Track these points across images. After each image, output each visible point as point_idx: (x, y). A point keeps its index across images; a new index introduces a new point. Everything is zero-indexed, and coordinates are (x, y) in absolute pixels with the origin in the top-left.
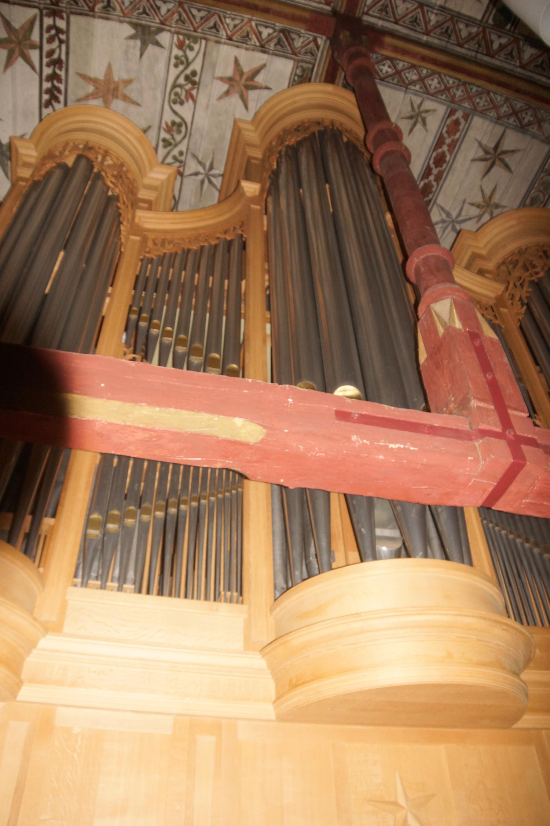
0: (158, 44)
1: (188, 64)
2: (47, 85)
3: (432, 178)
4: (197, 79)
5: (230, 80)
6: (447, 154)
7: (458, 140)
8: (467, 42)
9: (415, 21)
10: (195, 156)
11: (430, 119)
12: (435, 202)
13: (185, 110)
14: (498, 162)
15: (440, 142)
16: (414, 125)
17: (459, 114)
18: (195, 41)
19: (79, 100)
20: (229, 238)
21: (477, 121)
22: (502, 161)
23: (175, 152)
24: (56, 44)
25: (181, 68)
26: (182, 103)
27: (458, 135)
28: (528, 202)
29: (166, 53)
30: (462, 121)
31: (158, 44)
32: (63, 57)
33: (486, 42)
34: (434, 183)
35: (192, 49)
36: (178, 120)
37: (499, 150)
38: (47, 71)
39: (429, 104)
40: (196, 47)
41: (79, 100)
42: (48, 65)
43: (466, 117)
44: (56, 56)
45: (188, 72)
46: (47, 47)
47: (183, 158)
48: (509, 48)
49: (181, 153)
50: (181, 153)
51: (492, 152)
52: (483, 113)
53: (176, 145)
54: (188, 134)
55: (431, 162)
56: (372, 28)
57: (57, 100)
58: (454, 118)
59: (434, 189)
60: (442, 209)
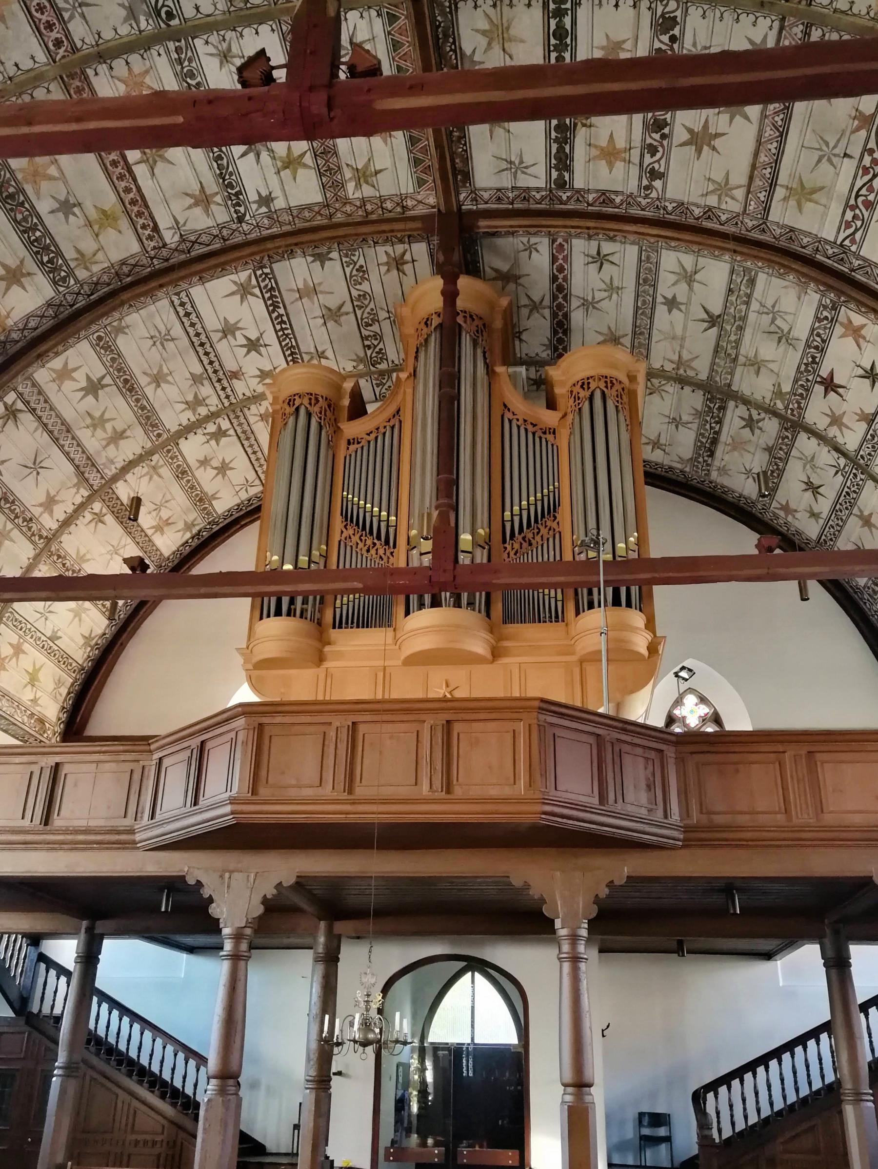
0: (331, 259)
1: (355, 263)
2: (269, 302)
3: (560, 280)
4: (365, 269)
5: (387, 263)
9: (499, 199)
10: (382, 309)
13: (365, 286)
15: (554, 259)
16: (531, 253)
17: (560, 240)
18: (355, 250)
19: (292, 303)
20: (391, 423)
21: (575, 241)
22: (608, 260)
23: (368, 310)
24: (267, 280)
25: (351, 266)
26: (360, 284)
27: (566, 252)
29: (339, 262)
31: (331, 259)
32: (274, 285)
33: (556, 197)
35: (354, 255)
36: (362, 293)
37: (602, 255)
38: (267, 295)
39: (533, 240)
40: (357, 253)
41: (292, 303)
42: (266, 292)
44: (269, 286)
45: (357, 267)
46: (262, 285)
48: (575, 197)
50: (372, 310)
52: (578, 236)
53: (367, 307)
54: (372, 298)
55: (555, 271)
56: (470, 212)
57: (279, 307)
58: (558, 243)
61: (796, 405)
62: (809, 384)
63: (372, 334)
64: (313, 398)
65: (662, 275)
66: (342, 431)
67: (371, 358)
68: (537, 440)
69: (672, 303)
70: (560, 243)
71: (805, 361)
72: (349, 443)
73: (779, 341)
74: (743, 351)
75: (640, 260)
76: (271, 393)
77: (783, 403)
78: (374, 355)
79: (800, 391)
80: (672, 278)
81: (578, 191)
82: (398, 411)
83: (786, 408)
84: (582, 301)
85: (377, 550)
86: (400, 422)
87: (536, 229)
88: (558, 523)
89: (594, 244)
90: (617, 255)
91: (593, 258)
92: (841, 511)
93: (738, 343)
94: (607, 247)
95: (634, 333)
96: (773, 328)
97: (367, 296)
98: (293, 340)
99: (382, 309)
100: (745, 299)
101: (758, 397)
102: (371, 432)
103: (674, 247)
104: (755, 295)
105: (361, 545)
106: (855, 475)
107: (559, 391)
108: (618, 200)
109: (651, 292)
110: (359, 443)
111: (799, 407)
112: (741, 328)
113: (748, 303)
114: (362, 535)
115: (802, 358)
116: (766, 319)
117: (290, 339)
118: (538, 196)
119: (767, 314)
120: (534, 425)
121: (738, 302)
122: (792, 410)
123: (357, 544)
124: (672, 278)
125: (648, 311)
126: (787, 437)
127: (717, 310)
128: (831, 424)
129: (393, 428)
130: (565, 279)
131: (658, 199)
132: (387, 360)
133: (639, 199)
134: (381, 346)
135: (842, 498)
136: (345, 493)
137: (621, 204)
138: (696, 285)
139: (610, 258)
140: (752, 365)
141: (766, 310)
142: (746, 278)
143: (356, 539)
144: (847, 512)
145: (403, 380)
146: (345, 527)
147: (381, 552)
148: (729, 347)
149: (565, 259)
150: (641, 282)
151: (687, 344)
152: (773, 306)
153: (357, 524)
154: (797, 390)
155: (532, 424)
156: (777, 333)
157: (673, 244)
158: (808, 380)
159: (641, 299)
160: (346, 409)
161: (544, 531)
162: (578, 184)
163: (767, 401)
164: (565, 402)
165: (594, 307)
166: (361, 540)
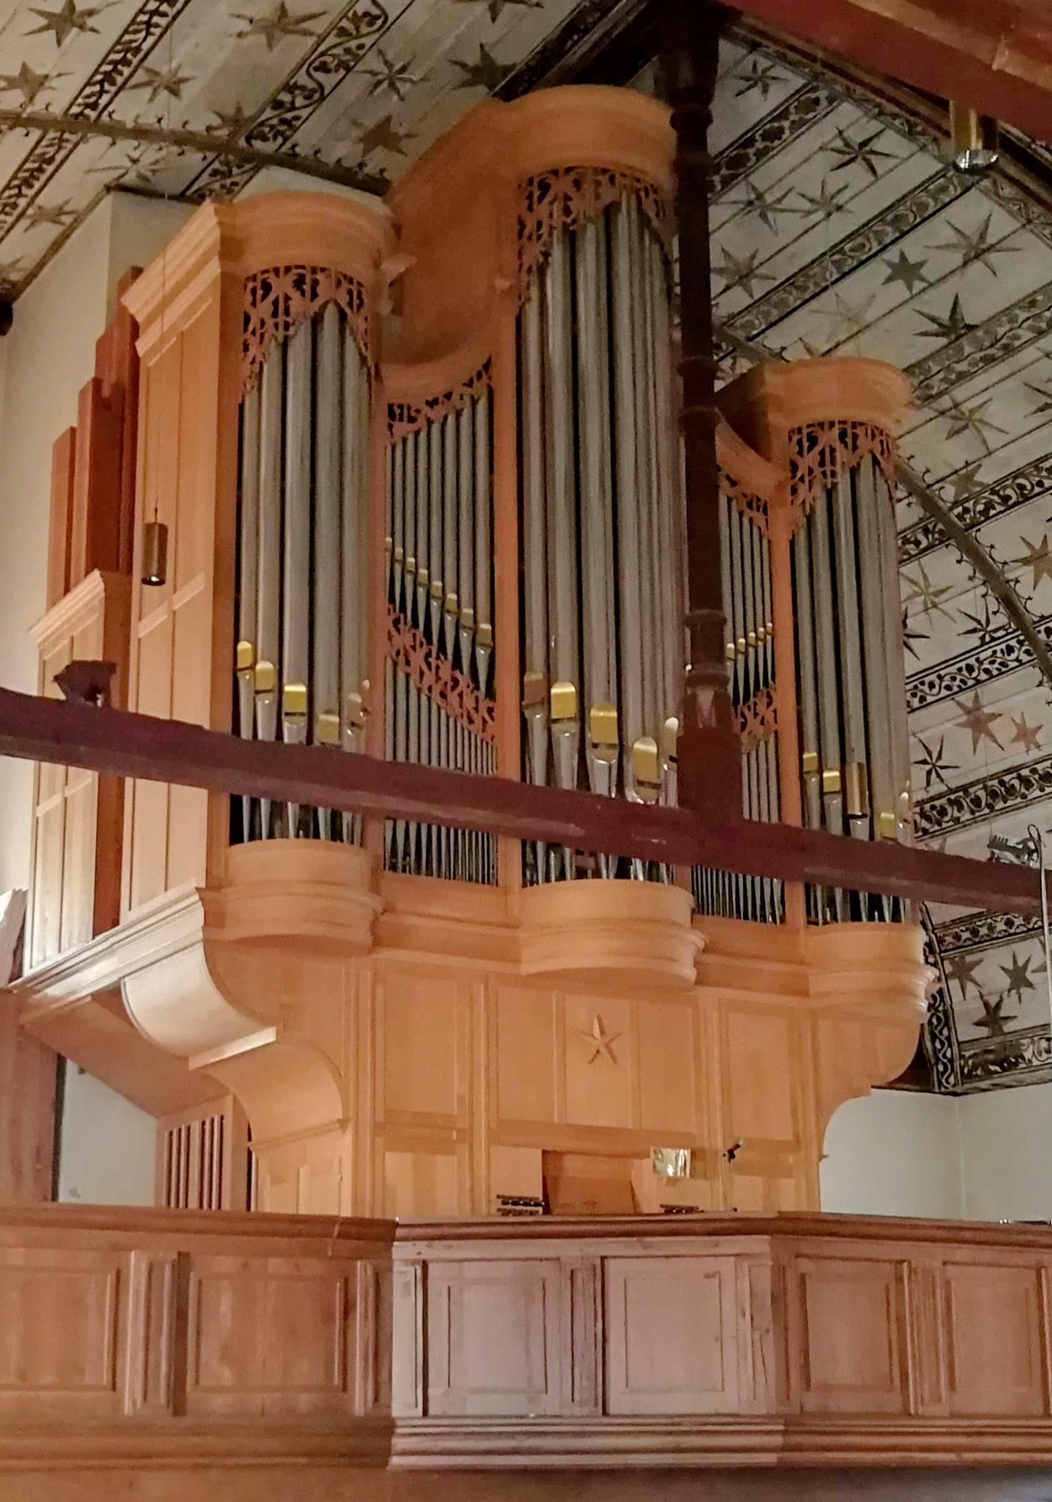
3: (751, 151)
6: (787, 133)
7: (809, 120)
11: (774, 88)
17: (822, 94)
23: (353, 44)
27: (811, 115)
30: (824, 103)
34: (754, 158)
43: (831, 100)
49: (361, 47)
51: (856, 147)
52: (859, 102)
59: (749, 164)
61: (980, 507)
62: (1037, 490)
63: (311, 85)
64: (354, 288)
67: (262, 124)
68: (735, 516)
69: (905, 271)
73: (1041, 410)
74: (959, 393)
75: (923, 186)
76: (220, 224)
77: (957, 494)
78: (275, 121)
79: (1009, 492)
80: (949, 236)
82: (487, 366)
83: (956, 504)
84: (753, 196)
85: (461, 695)
87: (798, 57)
88: (775, 711)
89: (875, 126)
90: (891, 162)
92: (932, 685)
93: (962, 376)
94: (891, 142)
95: (790, 281)
98: (151, 40)
100: (1043, 325)
101: (918, 466)
105: (429, 677)
106: (1010, 650)
107: (775, 419)
109: (888, 240)
110: (412, 420)
111: (985, 513)
112: (990, 360)
114: (428, 655)
117: (148, 33)
120: (734, 483)
121: (1025, 325)
122: (966, 510)
123: (422, 674)
124: (949, 236)
125: (851, 263)
126: (917, 543)
127: (972, 314)
128: (1025, 561)
129: (474, 402)
130: (761, 154)
132: (286, 139)
134: (304, 113)
135: (953, 669)
138: (977, 265)
140: (954, 418)
143: (417, 658)
144: (944, 693)
146: (396, 623)
147: (469, 702)
148: (941, 375)
149: (795, 125)
151: (862, 338)
153: (415, 624)
154: (1005, 488)
155: (728, 478)
157: (1008, 190)
158: (1040, 484)
159: (860, 240)
161: (753, 723)
163: (929, 479)
164: (781, 446)
165: (763, 216)
166: (429, 665)
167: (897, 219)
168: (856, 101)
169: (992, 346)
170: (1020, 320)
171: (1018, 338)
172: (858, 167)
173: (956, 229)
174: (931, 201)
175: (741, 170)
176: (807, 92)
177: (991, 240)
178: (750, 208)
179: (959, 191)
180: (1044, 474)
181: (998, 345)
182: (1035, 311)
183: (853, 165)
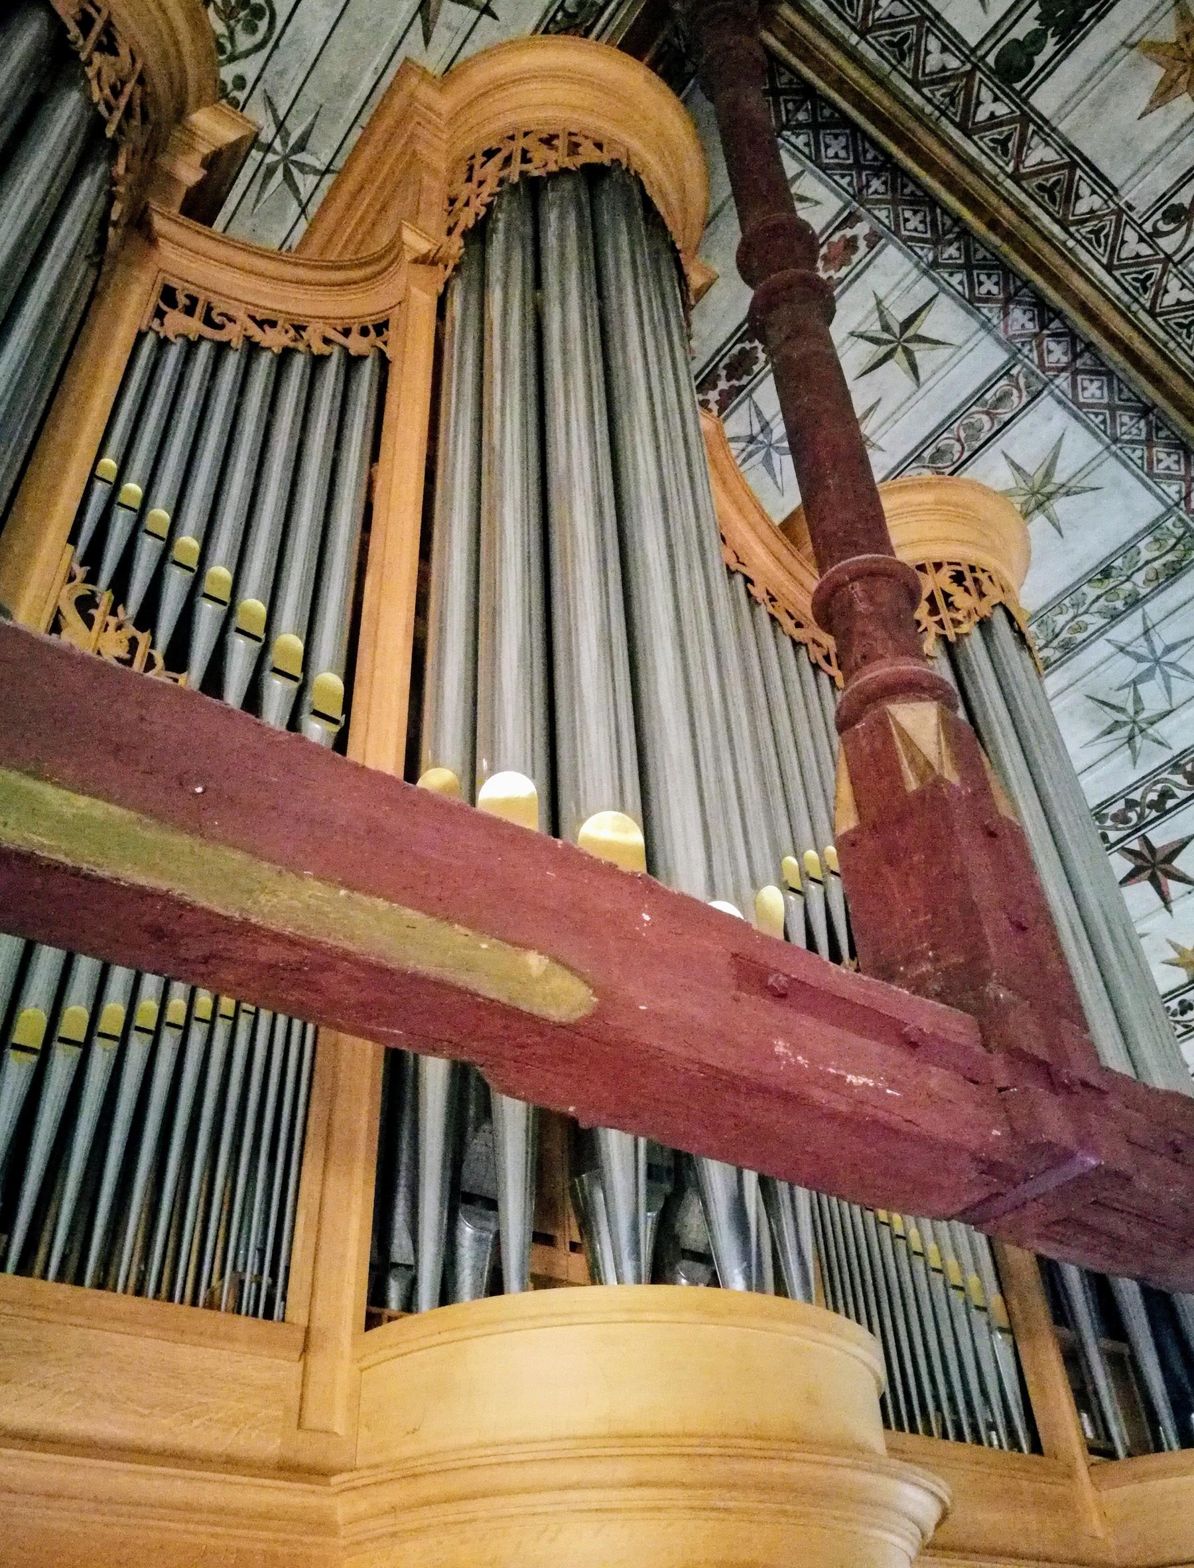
8: (932, 82)
10: (269, 102)
12: (749, 395)
14: (900, 355)
17: (861, 229)
21: (892, 256)
22: (908, 353)
28: (927, 454)
30: (862, 245)
43: (873, 240)
47: (241, 96)
49: (240, 82)
50: (240, 82)
51: (896, 329)
53: (233, 58)
59: (756, 368)
60: (759, 414)
65: (992, 454)
66: (151, 239)
70: (854, 239)
71: (1136, 796)
72: (168, 295)
73: (1109, 732)
75: (977, 397)
81: (1025, 119)
84: (757, 428)
86: (384, 364)
89: (925, 288)
90: (942, 353)
91: (886, 328)
96: (1124, 698)
97: (263, 25)
99: (269, 102)
100: (1119, 604)
102: (273, 324)
103: (1080, 406)
104: (1154, 609)
108: (1088, 202)
113: (1115, 617)
115: (1133, 788)
116: (1127, 668)
118: (934, 61)
119: (1139, 659)
131: (1168, 258)
133: (1130, 235)
136: (109, 464)
137: (1082, 222)
139: (921, 353)
141: (1144, 650)
142: (1170, 557)
145: (408, 257)
150: (927, 454)
152: (1169, 649)
156: (1121, 710)
157: (1093, 390)
160: (184, 191)
162: (1045, 100)
167: (939, 454)
168: (905, 240)
169: (1046, 646)
170: (1088, 602)
171: (1081, 628)
172: (895, 369)
173: (1013, 463)
174: (985, 418)
175: (745, 380)
176: (838, 228)
177: (1059, 477)
178: (751, 447)
179: (1025, 400)
180: (1109, 823)
181: (1055, 643)
182: (1111, 583)
183: (890, 364)
